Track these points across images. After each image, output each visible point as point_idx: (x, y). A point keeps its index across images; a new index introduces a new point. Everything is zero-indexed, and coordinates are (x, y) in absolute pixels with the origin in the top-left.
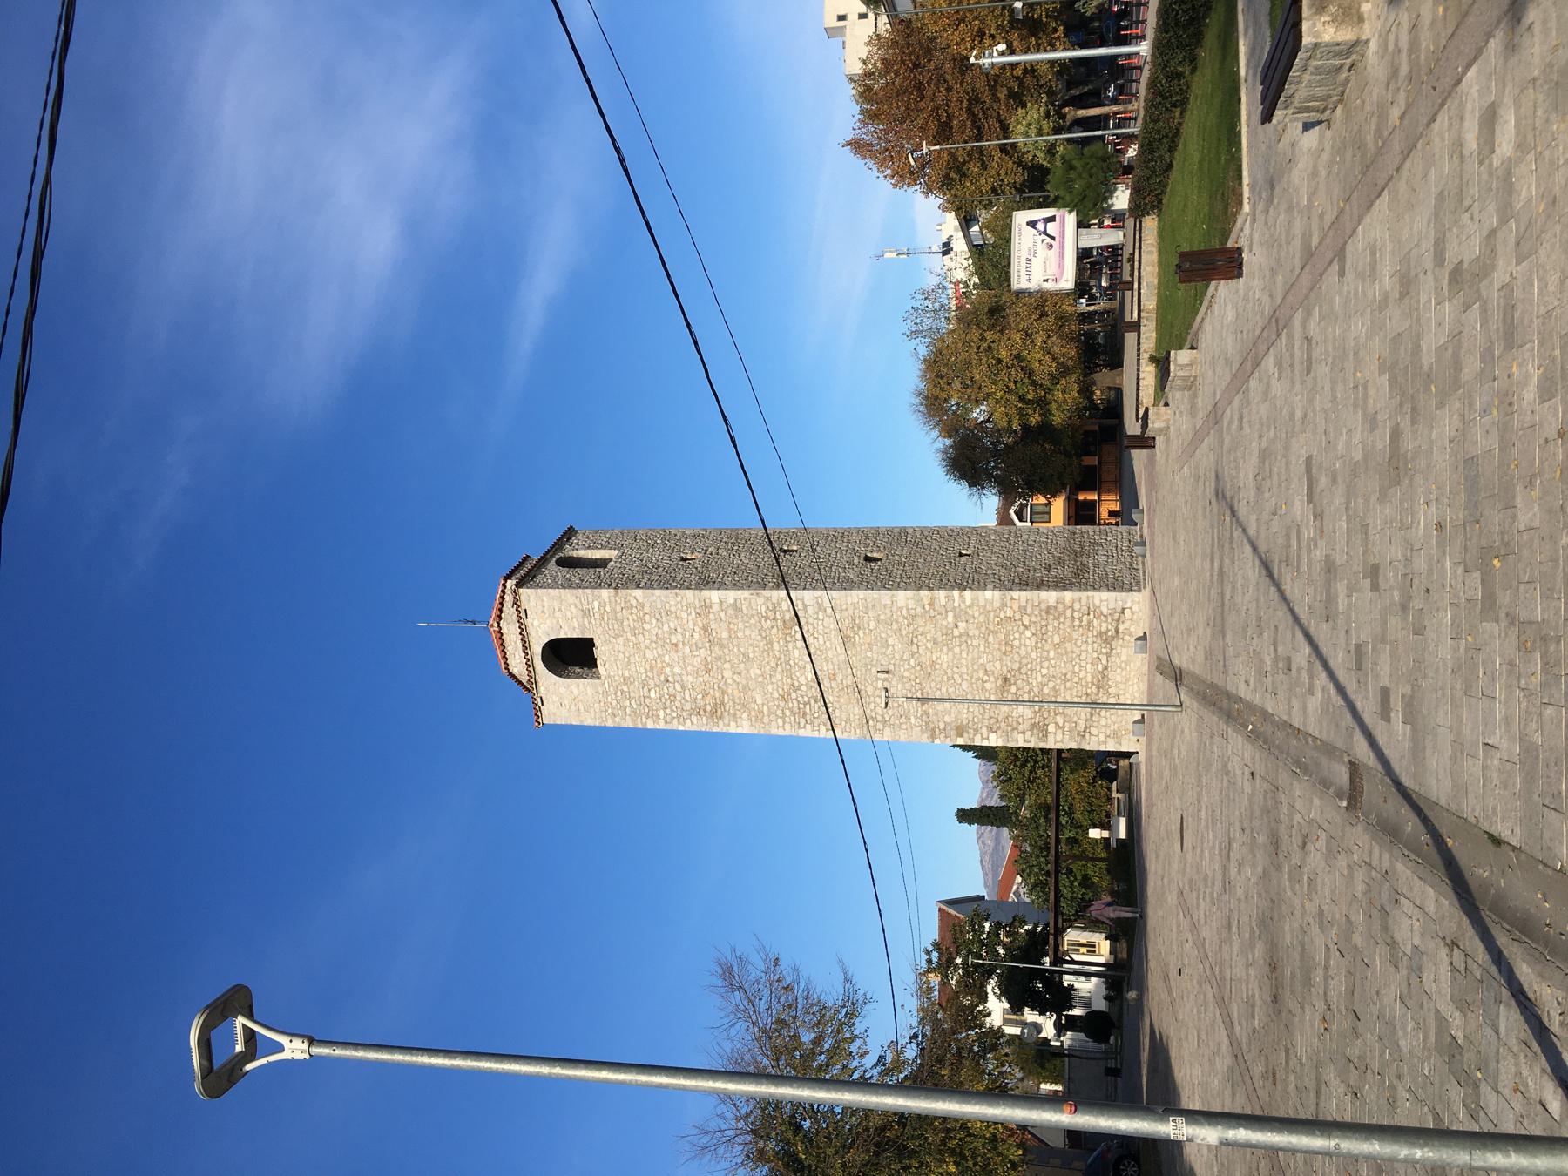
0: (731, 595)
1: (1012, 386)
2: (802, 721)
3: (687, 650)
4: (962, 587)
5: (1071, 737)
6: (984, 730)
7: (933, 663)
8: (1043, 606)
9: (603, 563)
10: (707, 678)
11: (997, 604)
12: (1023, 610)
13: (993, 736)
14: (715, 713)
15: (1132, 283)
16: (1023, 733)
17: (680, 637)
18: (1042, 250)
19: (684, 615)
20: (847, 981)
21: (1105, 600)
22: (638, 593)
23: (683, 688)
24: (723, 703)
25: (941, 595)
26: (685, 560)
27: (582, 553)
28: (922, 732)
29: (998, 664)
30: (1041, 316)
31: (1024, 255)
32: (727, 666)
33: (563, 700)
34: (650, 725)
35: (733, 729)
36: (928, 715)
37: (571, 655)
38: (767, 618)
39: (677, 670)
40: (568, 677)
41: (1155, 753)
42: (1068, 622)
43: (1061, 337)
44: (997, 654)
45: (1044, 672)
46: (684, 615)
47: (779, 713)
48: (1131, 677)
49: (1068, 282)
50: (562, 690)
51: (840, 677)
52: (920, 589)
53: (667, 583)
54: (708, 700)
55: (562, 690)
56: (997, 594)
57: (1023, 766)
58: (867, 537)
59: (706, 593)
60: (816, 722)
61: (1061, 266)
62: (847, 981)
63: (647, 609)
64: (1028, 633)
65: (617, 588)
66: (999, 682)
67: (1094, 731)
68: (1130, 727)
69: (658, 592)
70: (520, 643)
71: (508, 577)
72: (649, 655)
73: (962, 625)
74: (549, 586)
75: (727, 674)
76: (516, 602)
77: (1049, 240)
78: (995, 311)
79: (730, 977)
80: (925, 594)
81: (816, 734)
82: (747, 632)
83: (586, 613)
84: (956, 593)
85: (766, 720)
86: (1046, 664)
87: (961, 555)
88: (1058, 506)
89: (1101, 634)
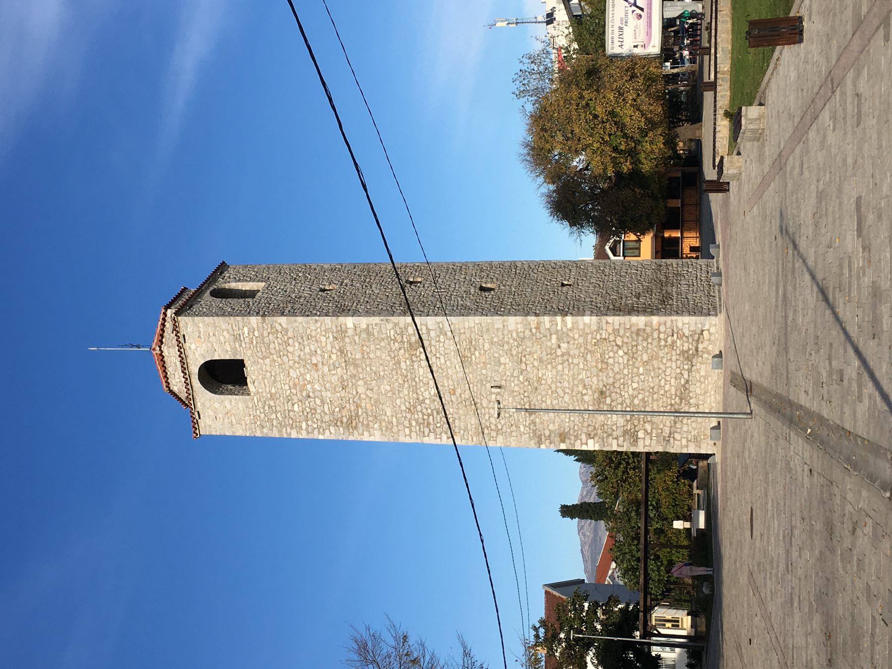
0: (364, 321)
1: (607, 138)
2: (427, 431)
3: (326, 369)
4: (564, 313)
5: (658, 442)
6: (584, 436)
7: (539, 379)
8: (634, 329)
9: (252, 294)
10: (343, 393)
11: (594, 328)
12: (616, 332)
13: (591, 442)
14: (351, 424)
15: (710, 48)
16: (617, 438)
17: (319, 358)
18: (632, 18)
19: (323, 339)
20: (466, 654)
21: (686, 323)
22: (283, 320)
23: (323, 402)
24: (357, 415)
25: (546, 319)
26: (323, 290)
27: (233, 285)
28: (530, 439)
29: (595, 379)
30: (632, 77)
31: (617, 24)
32: (361, 383)
33: (217, 414)
34: (294, 435)
35: (366, 437)
36: (534, 423)
37: (224, 375)
38: (395, 340)
39: (317, 387)
40: (222, 393)
41: (729, 454)
42: (655, 343)
43: (649, 96)
44: (594, 371)
45: (635, 385)
46: (323, 339)
47: (406, 423)
48: (709, 389)
49: (654, 47)
50: (217, 405)
51: (458, 391)
52: (528, 314)
53: (308, 311)
54: (345, 412)
55: (217, 405)
56: (594, 318)
57: (617, 468)
58: (482, 270)
59: (342, 319)
60: (438, 431)
61: (649, 34)
62: (466, 654)
63: (290, 334)
64: (621, 353)
65: (264, 315)
66: (596, 395)
67: (677, 436)
68: (708, 432)
69: (300, 319)
70: (179, 364)
71: (168, 307)
72: (293, 374)
73: (564, 346)
74: (205, 315)
75: (361, 390)
76: (176, 329)
77: (638, 11)
78: (592, 73)
80: (531, 319)
81: (438, 442)
82: (378, 353)
83: (237, 338)
84: (559, 318)
85: (395, 429)
86: (636, 379)
87: (563, 285)
88: (647, 243)
89: (683, 352)
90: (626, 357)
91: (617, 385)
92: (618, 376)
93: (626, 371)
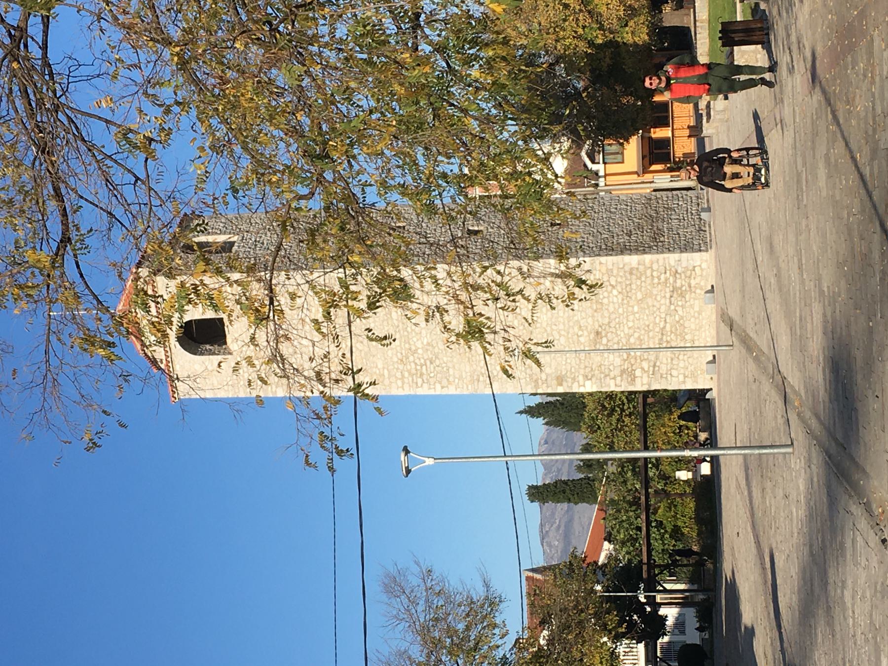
16: (614, 378)
42: (649, 281)
45: (630, 324)
64: (615, 292)
67: (674, 373)
79: (394, 586)
86: (631, 318)
90: (620, 297)
91: (612, 325)
92: (613, 316)
93: (621, 311)
